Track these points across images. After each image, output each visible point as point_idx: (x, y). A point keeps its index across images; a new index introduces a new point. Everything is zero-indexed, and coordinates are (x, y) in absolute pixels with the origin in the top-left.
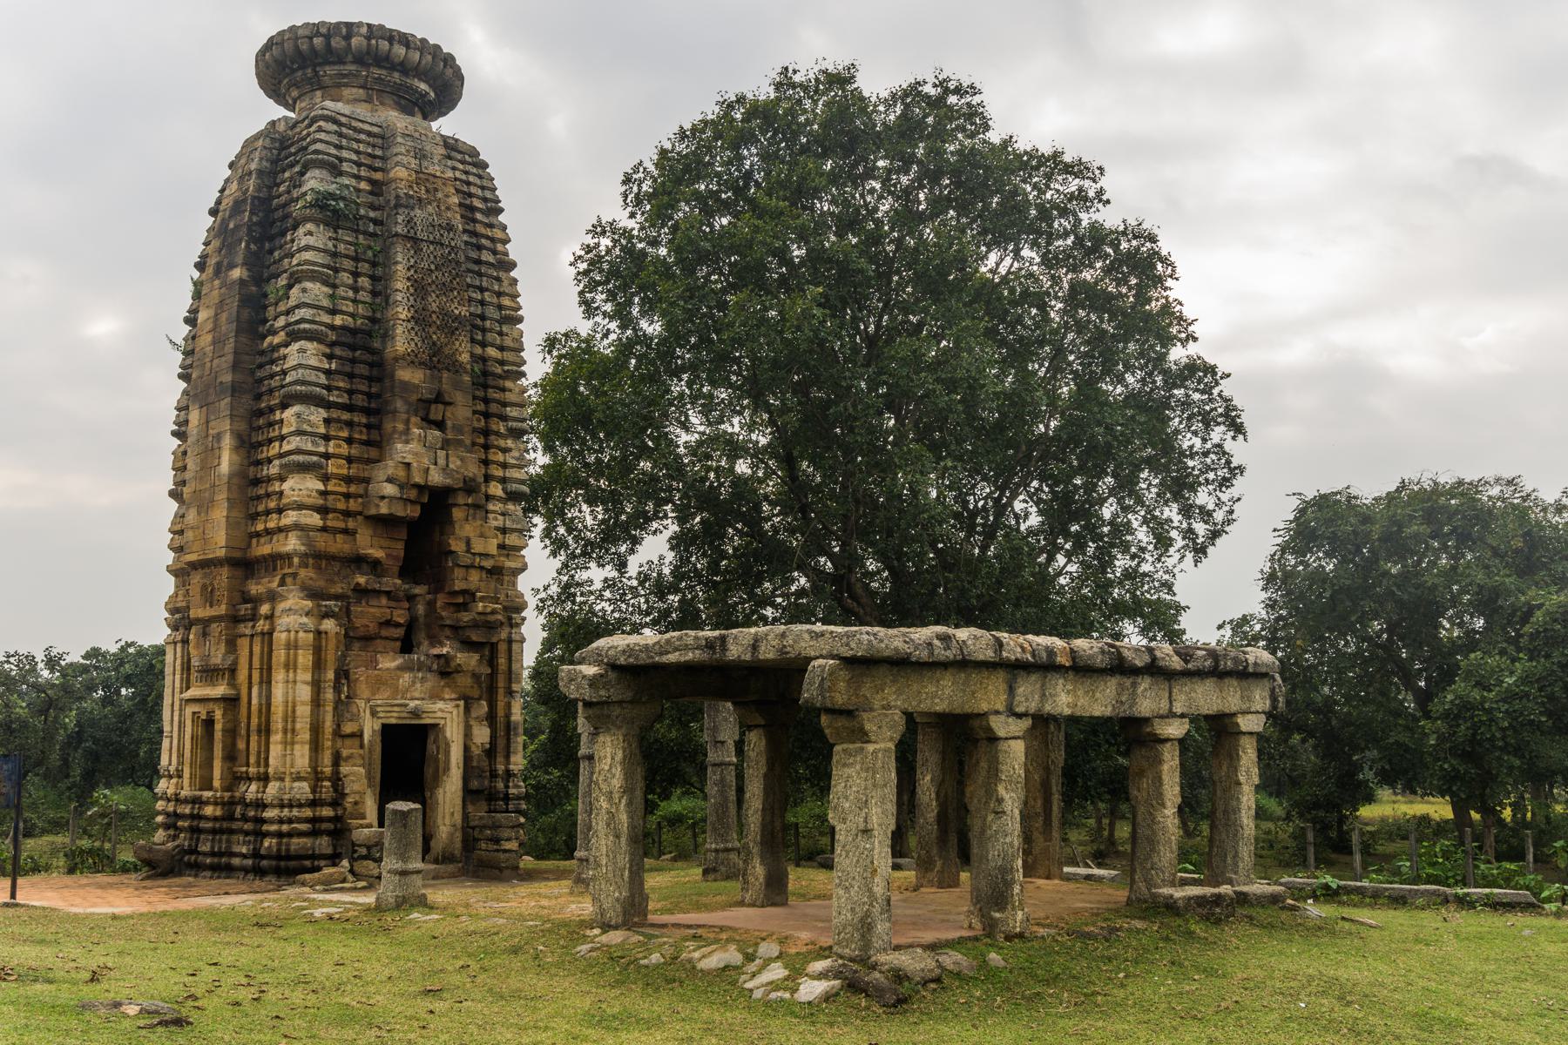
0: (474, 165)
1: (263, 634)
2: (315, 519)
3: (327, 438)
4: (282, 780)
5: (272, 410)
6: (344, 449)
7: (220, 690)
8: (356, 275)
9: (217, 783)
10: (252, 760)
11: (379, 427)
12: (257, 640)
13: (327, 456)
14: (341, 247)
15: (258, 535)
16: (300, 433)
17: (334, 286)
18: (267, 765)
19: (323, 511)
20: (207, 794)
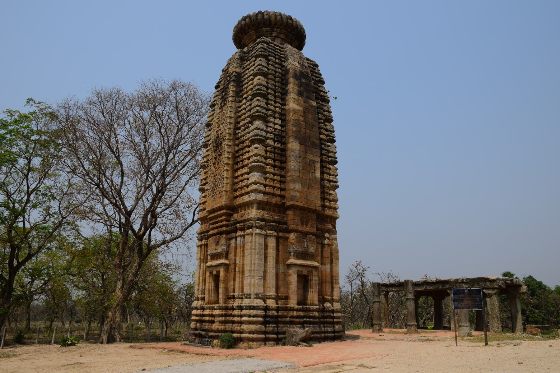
1: (241, 236)
2: (262, 188)
4: (250, 298)
6: (272, 162)
7: (223, 261)
8: (275, 97)
9: (221, 301)
10: (237, 290)
11: (285, 155)
12: (239, 239)
13: (267, 164)
14: (270, 86)
16: (256, 155)
18: (242, 291)
19: (265, 186)
20: (216, 306)
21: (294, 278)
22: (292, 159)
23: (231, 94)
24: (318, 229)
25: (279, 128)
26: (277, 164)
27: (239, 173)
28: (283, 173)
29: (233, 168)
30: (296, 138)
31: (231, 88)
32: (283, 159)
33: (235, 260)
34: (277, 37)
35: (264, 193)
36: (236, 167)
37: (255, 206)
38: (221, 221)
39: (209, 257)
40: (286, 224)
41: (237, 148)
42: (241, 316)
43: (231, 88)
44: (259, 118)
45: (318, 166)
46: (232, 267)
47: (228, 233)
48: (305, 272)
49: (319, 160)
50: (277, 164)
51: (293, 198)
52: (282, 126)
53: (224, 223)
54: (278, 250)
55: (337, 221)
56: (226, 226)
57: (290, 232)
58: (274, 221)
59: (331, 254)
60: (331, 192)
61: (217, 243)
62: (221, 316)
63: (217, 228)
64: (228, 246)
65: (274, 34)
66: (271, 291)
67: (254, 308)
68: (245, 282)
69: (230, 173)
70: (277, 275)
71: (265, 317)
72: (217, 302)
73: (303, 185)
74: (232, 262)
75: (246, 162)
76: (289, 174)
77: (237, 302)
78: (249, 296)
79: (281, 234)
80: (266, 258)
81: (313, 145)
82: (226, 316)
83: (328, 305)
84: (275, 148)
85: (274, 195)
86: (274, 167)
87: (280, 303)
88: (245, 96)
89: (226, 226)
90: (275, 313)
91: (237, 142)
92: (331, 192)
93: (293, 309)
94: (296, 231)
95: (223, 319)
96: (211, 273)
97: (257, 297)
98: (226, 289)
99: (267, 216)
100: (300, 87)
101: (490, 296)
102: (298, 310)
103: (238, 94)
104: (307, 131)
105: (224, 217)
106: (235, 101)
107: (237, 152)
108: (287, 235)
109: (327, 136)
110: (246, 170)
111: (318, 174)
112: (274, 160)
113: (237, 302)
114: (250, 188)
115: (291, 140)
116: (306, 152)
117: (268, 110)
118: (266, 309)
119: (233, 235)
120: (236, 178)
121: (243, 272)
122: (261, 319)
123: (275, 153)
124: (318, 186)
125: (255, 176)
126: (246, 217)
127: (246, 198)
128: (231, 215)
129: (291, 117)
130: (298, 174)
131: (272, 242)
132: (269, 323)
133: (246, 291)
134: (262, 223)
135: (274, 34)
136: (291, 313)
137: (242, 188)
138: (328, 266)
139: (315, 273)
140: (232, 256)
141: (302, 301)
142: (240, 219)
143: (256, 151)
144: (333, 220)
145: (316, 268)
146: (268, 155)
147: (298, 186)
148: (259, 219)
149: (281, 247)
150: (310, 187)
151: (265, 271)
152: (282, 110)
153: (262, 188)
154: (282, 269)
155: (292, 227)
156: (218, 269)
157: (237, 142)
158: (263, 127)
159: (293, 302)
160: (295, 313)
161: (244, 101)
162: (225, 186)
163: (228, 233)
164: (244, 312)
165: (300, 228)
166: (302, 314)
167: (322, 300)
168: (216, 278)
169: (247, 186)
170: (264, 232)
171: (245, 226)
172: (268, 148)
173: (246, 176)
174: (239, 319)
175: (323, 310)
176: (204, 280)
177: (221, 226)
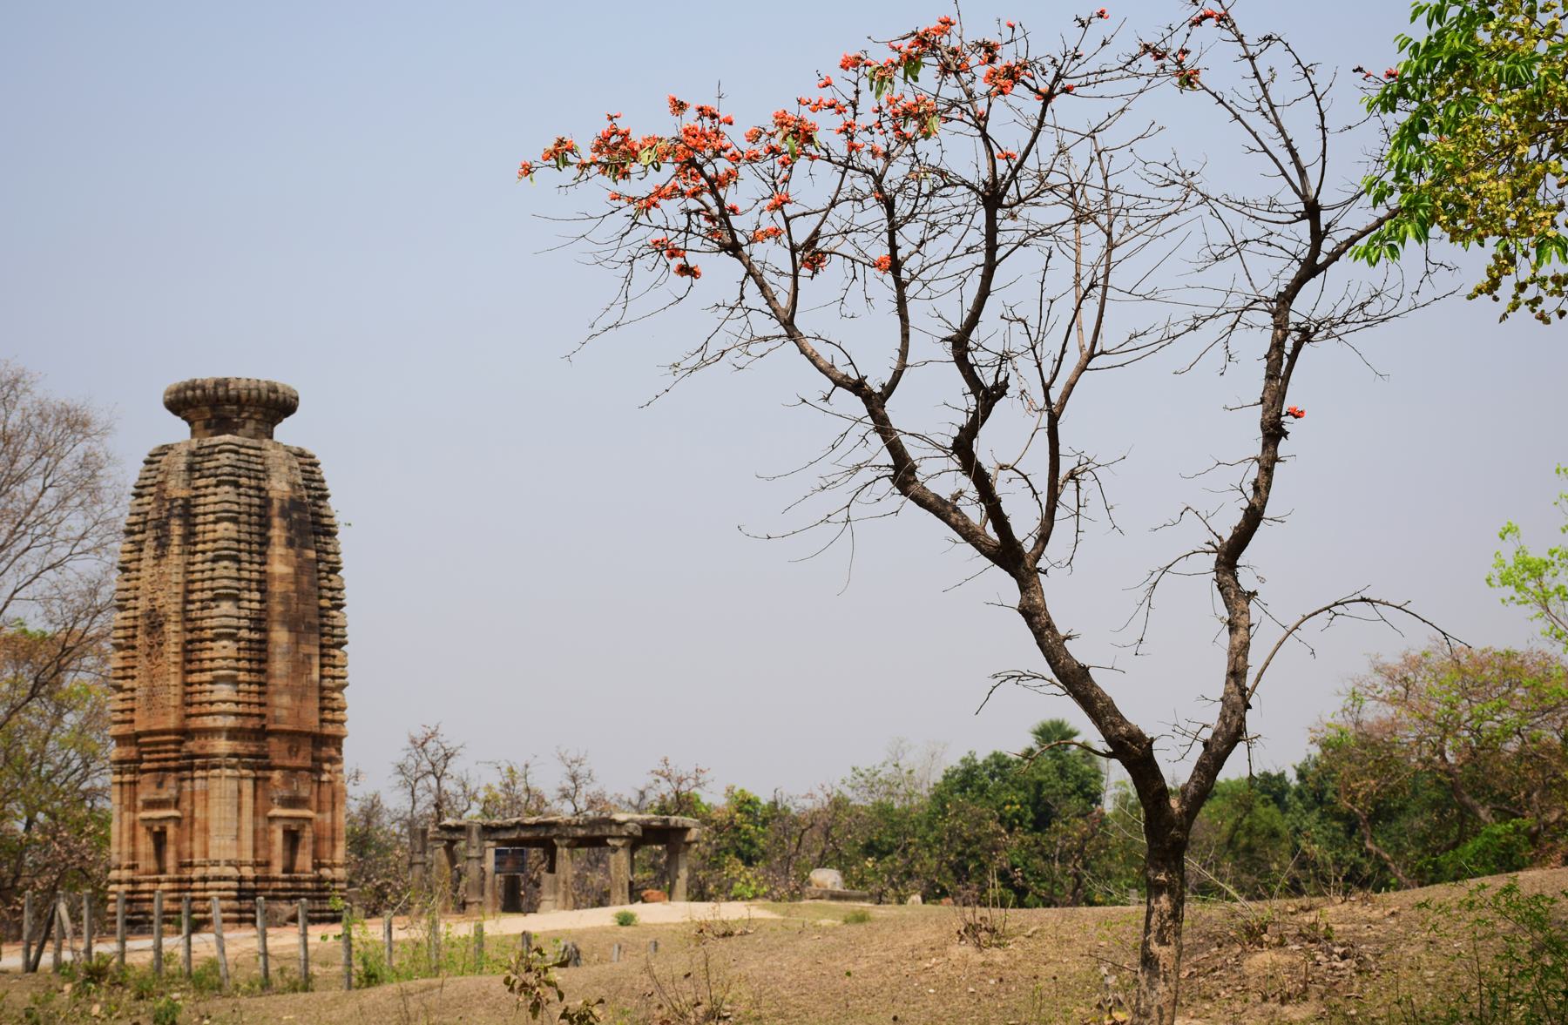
0: (312, 464)
3: (238, 660)
5: (202, 641)
7: (172, 812)
11: (265, 650)
13: (238, 670)
15: (191, 716)
17: (239, 561)
20: (162, 877)
21: (278, 836)
22: (278, 658)
23: (176, 540)
24: (314, 760)
25: (255, 605)
26: (255, 666)
27: (195, 678)
28: (263, 679)
29: (183, 668)
30: (283, 623)
31: (176, 529)
32: (263, 656)
33: (193, 812)
34: (249, 418)
35: (236, 714)
36: (189, 667)
37: (224, 735)
38: (166, 751)
39: (140, 804)
40: (266, 757)
41: (189, 636)
42: (205, 890)
43: (176, 529)
44: (228, 597)
45: (316, 661)
46: (186, 821)
47: (177, 770)
48: (294, 828)
49: (316, 651)
50: (255, 666)
51: (276, 721)
52: (261, 602)
53: (173, 755)
54: (255, 797)
55: (345, 741)
56: (176, 759)
57: (272, 768)
58: (250, 756)
59: (333, 795)
60: (336, 695)
61: (160, 785)
62: (173, 891)
63: (158, 760)
64: (180, 790)
65: (245, 415)
66: (248, 856)
67: (225, 879)
68: (211, 843)
69: (179, 676)
70: (255, 832)
71: (239, 890)
72: (162, 871)
73: (293, 696)
74: (187, 814)
75: (207, 664)
76: (272, 681)
77: (197, 873)
78: (216, 863)
79: (260, 773)
80: (239, 809)
81: (310, 627)
82: (179, 891)
83: (326, 872)
84: (250, 641)
85: (249, 715)
86: (250, 671)
87: (260, 872)
88: (200, 547)
89: (176, 759)
90: (251, 885)
91: (189, 625)
92: (336, 695)
93: (276, 880)
94: (282, 768)
95: (175, 895)
96: (149, 829)
97: (229, 863)
98: (179, 854)
99: (241, 749)
100: (289, 530)
101: (615, 849)
102: (284, 880)
103: (189, 537)
104: (301, 606)
105: (172, 747)
106: (183, 553)
107: (191, 642)
108: (268, 773)
109: (332, 599)
110: (207, 676)
111: (316, 676)
112: (250, 660)
113: (197, 873)
114: (214, 708)
115: (276, 627)
116: (298, 643)
117: (239, 579)
118: (241, 880)
119: (187, 773)
120: (191, 684)
121: (206, 830)
122: (234, 894)
123: (250, 649)
124: (315, 694)
125: (224, 691)
126: (209, 750)
127: (209, 722)
128: (180, 743)
129: (277, 588)
130: (285, 681)
131: (248, 786)
132: (245, 898)
133: (212, 856)
134: (234, 760)
135: (245, 415)
136: (274, 885)
137: (201, 703)
138: (328, 816)
139: (308, 829)
140: (186, 805)
141: (289, 869)
142: (197, 750)
143: (224, 653)
144: (337, 741)
145: (309, 819)
146: (242, 654)
147: (285, 700)
148: (230, 755)
149: (260, 793)
150: (303, 697)
151: (239, 829)
152: (260, 572)
153: (233, 708)
154: (261, 823)
155: (277, 762)
156: (163, 823)
157: (189, 625)
158: (234, 611)
159: (277, 870)
160: (280, 885)
161: (199, 557)
162: (173, 697)
163: (177, 770)
164: (209, 885)
165: (288, 763)
166: (289, 885)
167: (318, 866)
168: (159, 839)
169: (212, 703)
170: (237, 773)
171: (209, 762)
172: (242, 644)
173: (208, 687)
174: (202, 894)
175: (320, 880)
176: (133, 839)
177: (166, 760)
